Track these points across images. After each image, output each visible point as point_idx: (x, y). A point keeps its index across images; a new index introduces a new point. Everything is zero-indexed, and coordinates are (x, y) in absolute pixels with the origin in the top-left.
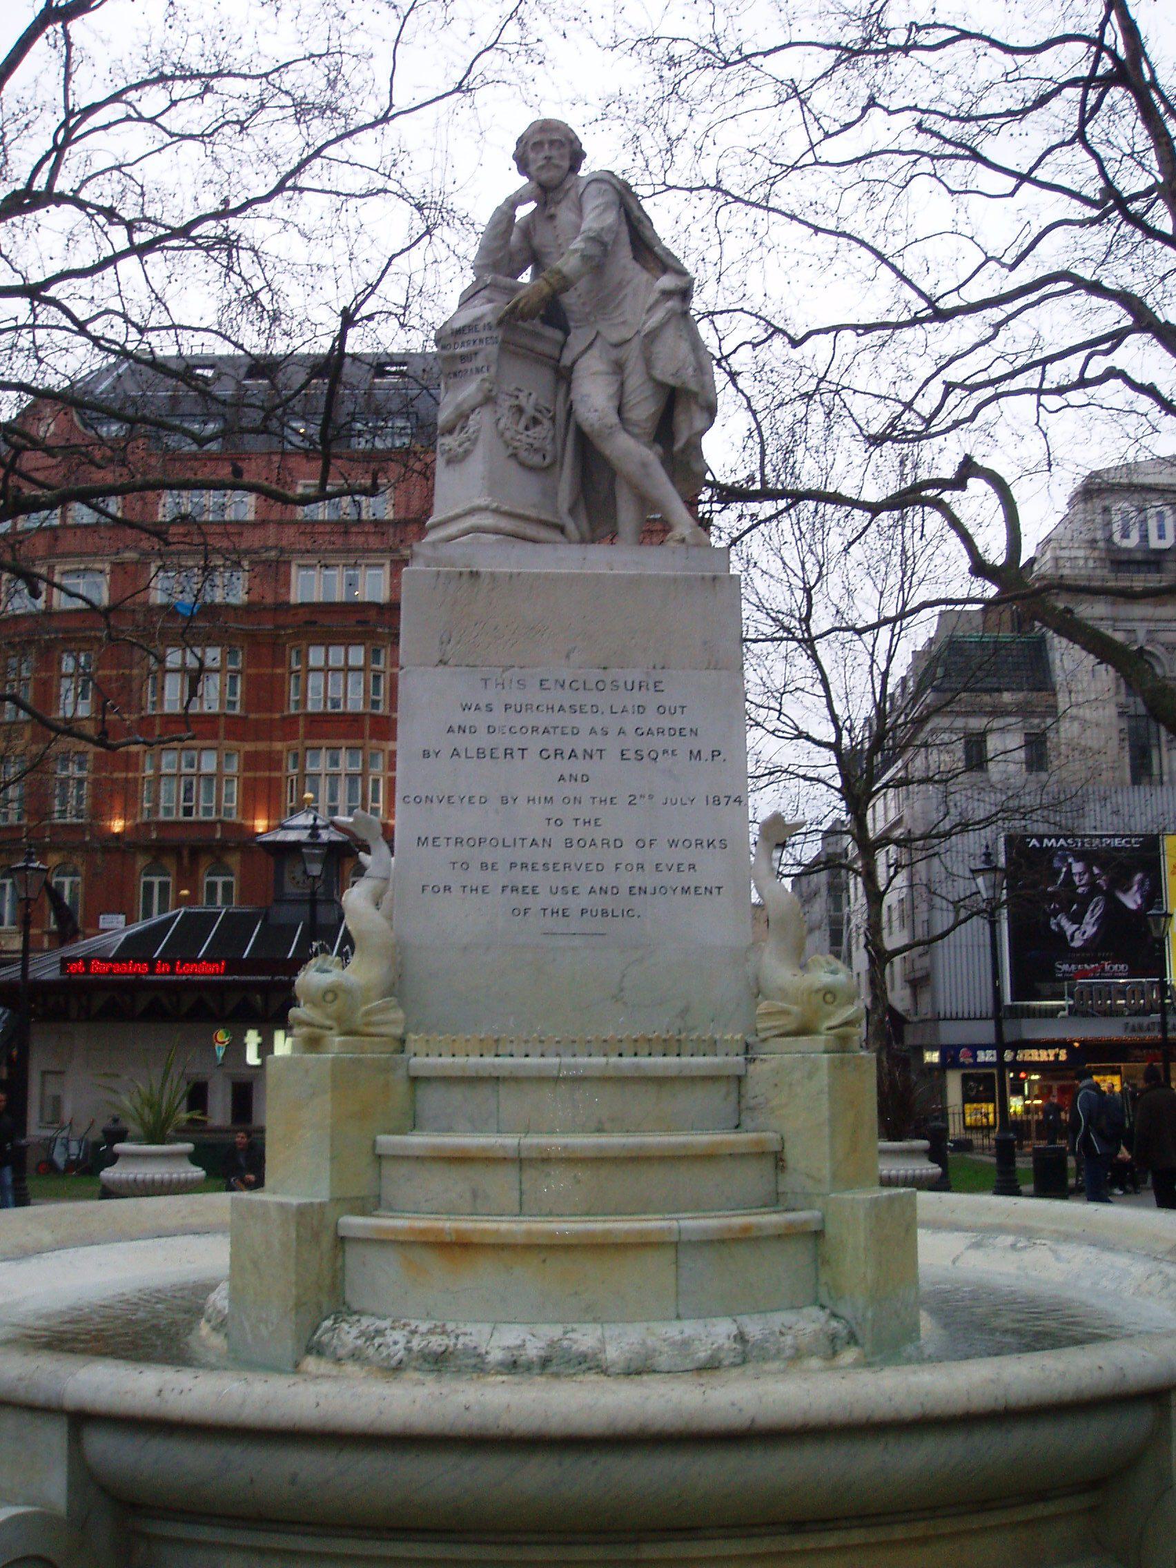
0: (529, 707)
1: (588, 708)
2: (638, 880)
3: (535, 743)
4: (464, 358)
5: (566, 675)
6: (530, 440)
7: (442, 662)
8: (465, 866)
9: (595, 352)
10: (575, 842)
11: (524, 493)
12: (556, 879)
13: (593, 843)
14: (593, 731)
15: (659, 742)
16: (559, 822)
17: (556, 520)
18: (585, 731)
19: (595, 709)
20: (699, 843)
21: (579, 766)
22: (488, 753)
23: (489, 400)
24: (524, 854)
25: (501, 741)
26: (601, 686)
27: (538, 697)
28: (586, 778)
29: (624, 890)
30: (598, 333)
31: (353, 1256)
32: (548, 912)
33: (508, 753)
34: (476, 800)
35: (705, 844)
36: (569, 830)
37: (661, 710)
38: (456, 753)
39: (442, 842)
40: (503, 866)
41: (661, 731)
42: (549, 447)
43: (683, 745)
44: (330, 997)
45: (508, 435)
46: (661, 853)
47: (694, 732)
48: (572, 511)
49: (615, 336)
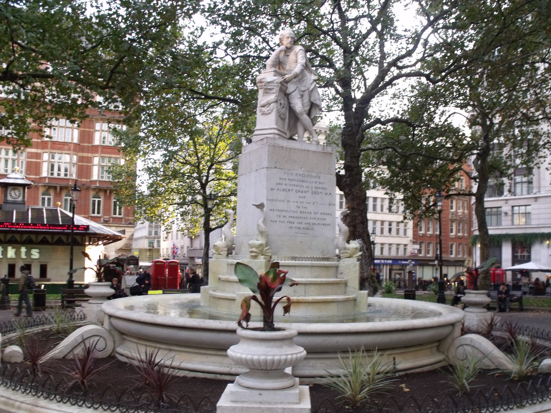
3: (295, 188)
4: (270, 89)
5: (301, 173)
7: (276, 168)
8: (280, 216)
9: (297, 91)
15: (320, 190)
16: (299, 207)
21: (303, 194)
23: (276, 102)
25: (289, 187)
27: (296, 178)
28: (305, 197)
33: (289, 190)
36: (302, 209)
43: (324, 192)
46: (319, 216)
49: (303, 89)
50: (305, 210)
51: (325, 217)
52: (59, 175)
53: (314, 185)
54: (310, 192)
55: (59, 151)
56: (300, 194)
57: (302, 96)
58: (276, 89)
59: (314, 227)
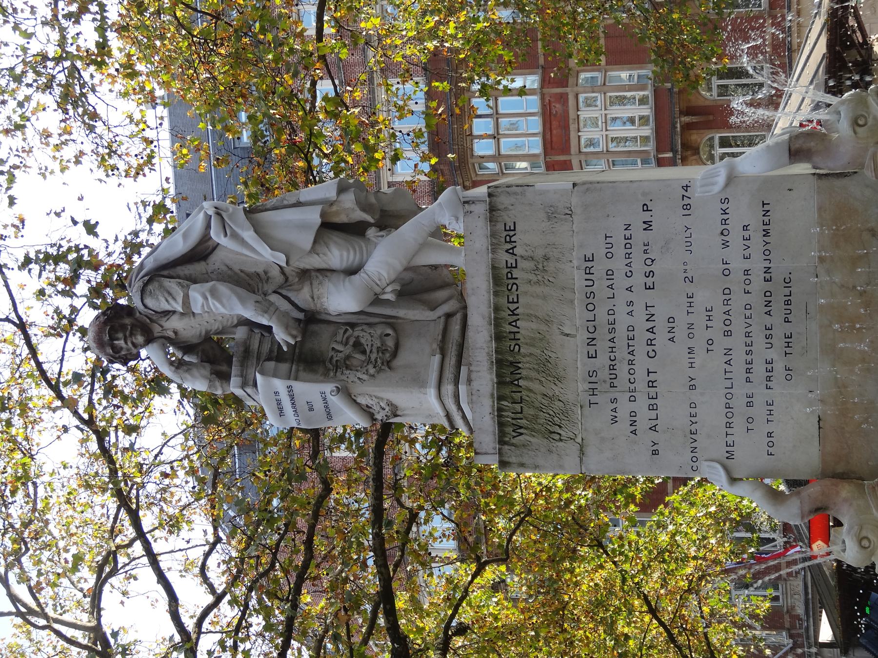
0: (612, 368)
1: (611, 318)
2: (757, 278)
3: (642, 363)
6: (375, 350)
8: (750, 420)
10: (727, 328)
13: (727, 313)
14: (630, 313)
17: (443, 319)
18: (629, 320)
19: (611, 312)
20: (724, 222)
21: (660, 323)
22: (653, 402)
26: (591, 307)
29: (768, 286)
30: (275, 292)
32: (788, 350)
33: (651, 384)
34: (693, 411)
35: (725, 217)
36: (716, 333)
37: (609, 255)
38: (653, 428)
39: (730, 439)
40: (748, 389)
41: (628, 256)
42: (379, 332)
43: (639, 236)
44: (865, 543)
45: (372, 371)
47: (628, 227)
48: (433, 308)
50: (718, 316)
51: (735, 227)
53: (621, 282)
55: (573, 127)
56: (661, 338)
59: (778, 276)
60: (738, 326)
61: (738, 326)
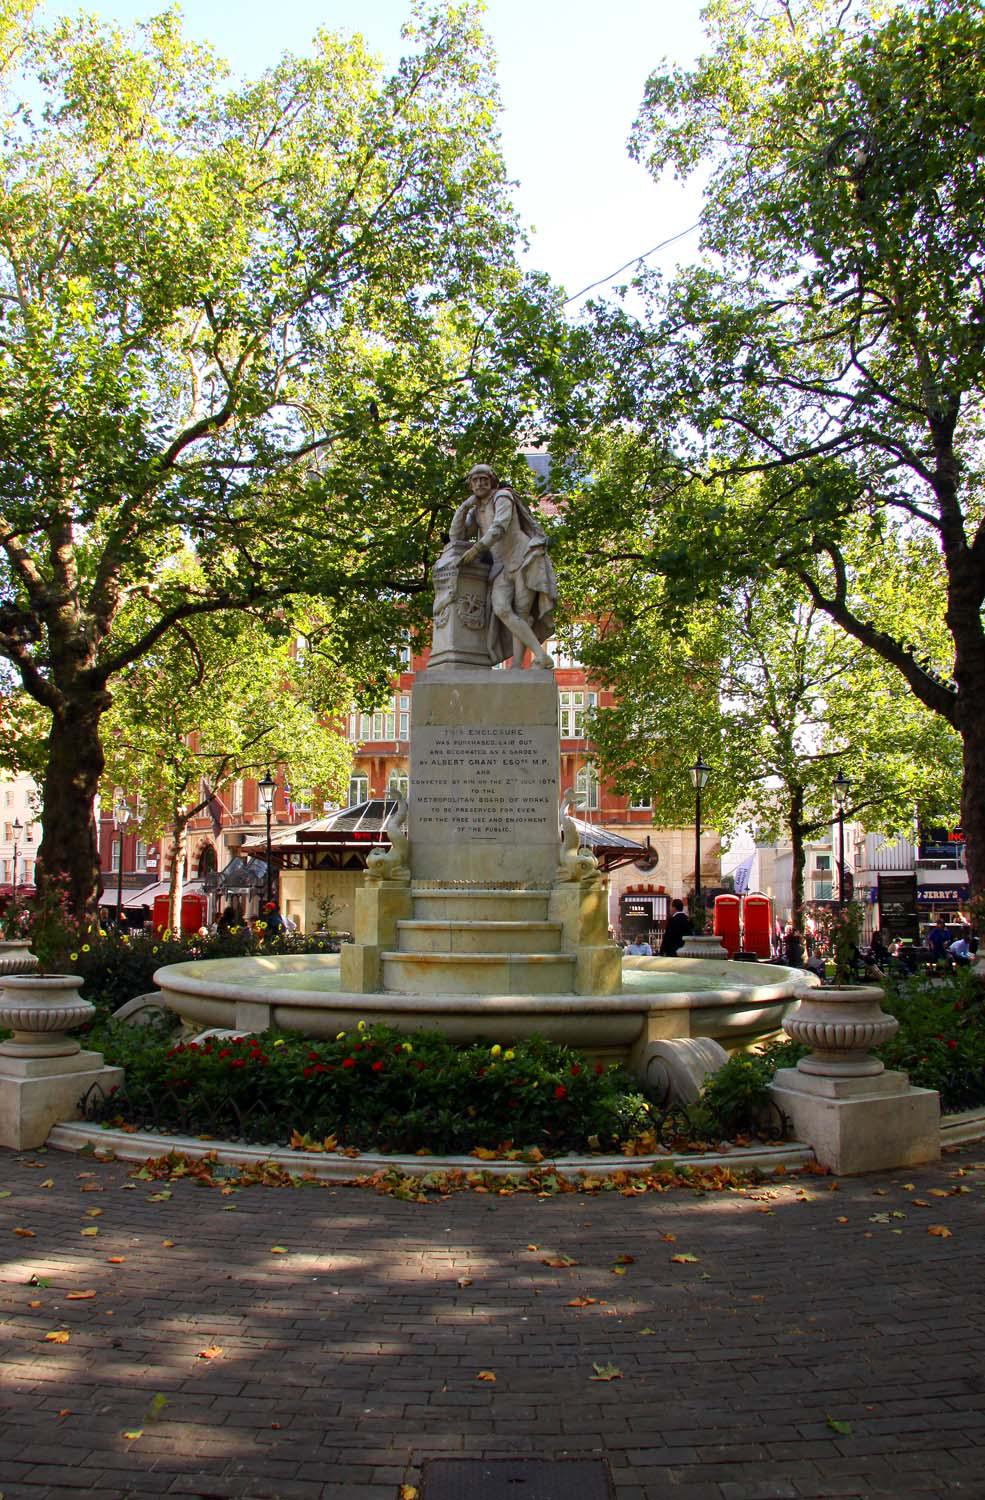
2: (509, 815)
3: (467, 757)
11: (471, 641)
12: (477, 816)
19: (493, 743)
21: (485, 767)
23: (453, 601)
24: (461, 805)
31: (386, 964)
33: (456, 762)
36: (481, 795)
43: (530, 758)
51: (533, 805)
52: (566, 732)
54: (499, 763)
57: (512, 583)
58: (452, 581)
60: (484, 805)
61: (484, 805)
